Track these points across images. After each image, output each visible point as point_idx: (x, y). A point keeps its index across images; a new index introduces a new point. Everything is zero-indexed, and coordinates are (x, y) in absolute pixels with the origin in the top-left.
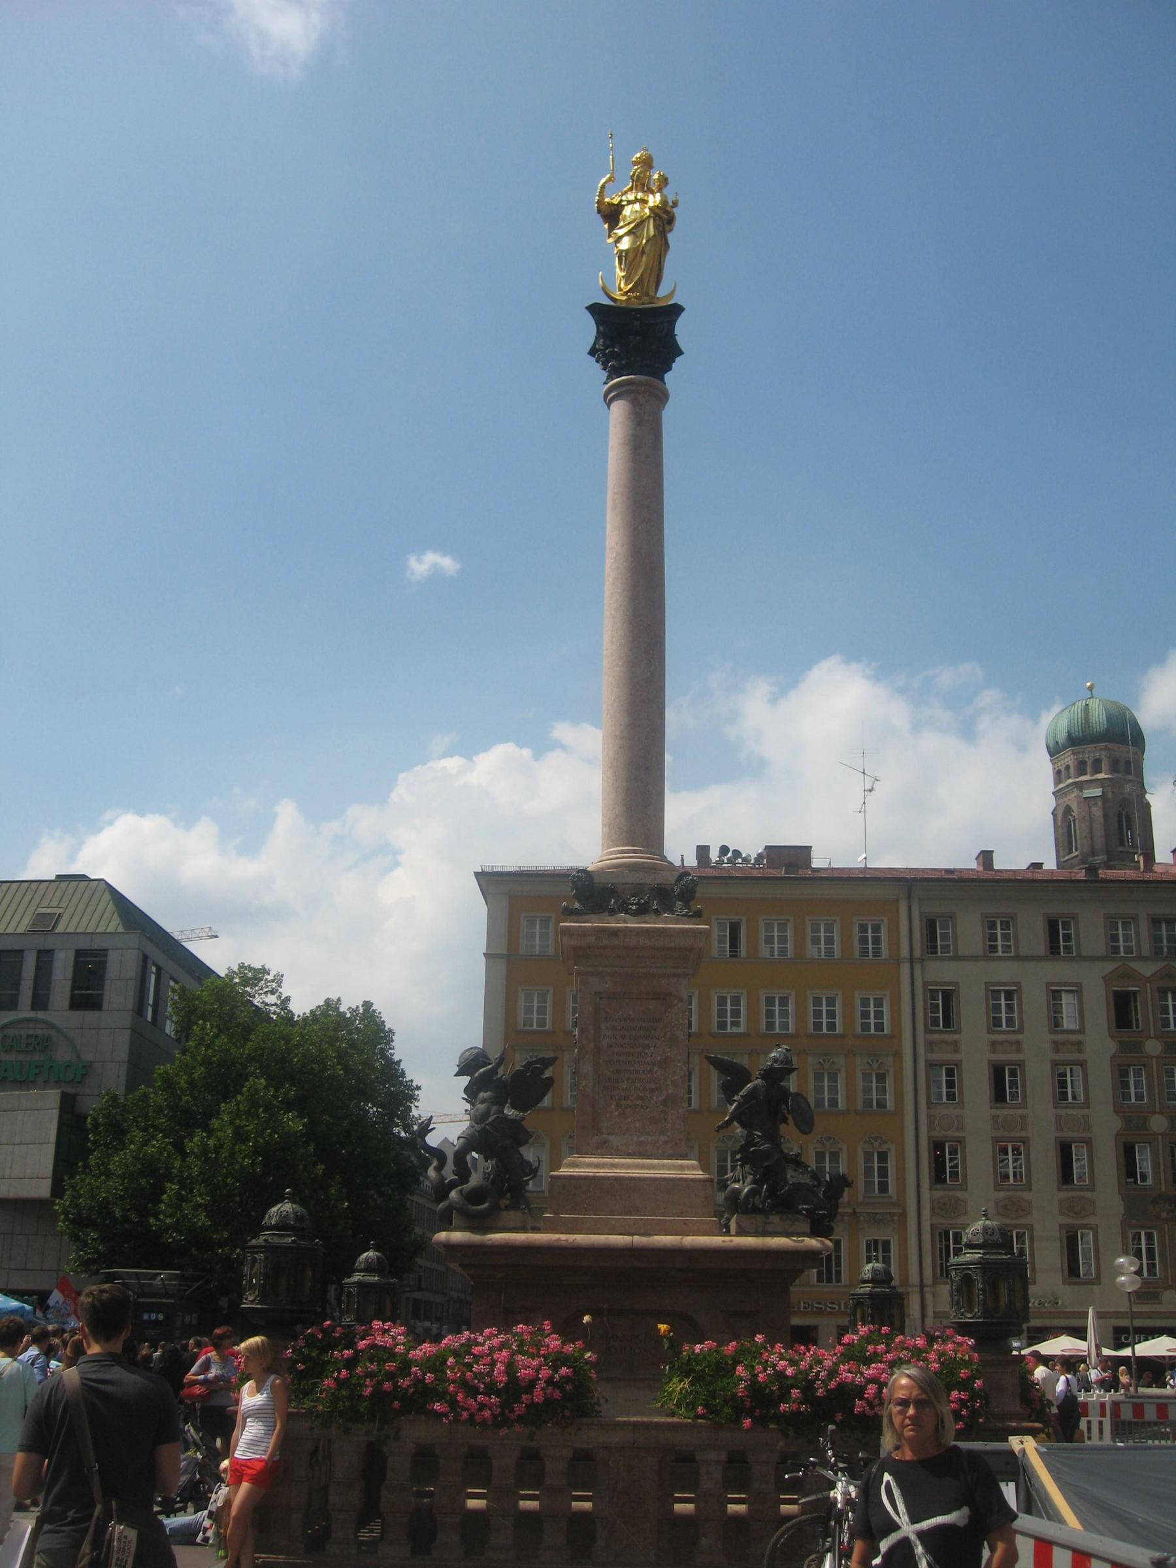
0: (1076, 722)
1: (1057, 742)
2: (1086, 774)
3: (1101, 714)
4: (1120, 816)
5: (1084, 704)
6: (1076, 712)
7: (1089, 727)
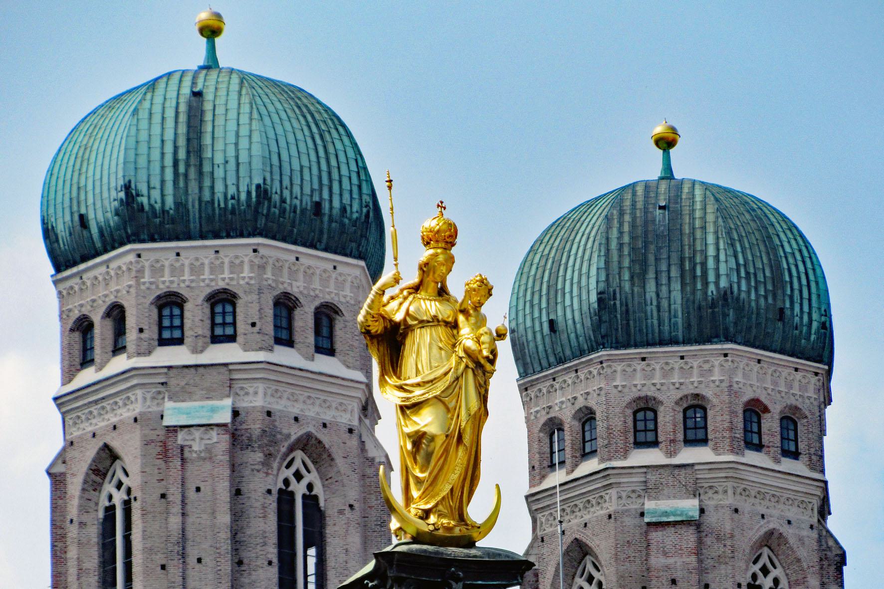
0: (156, 155)
1: (83, 221)
2: (180, 341)
3: (244, 131)
4: (285, 498)
5: (186, 91)
6: (157, 119)
7: (201, 173)
